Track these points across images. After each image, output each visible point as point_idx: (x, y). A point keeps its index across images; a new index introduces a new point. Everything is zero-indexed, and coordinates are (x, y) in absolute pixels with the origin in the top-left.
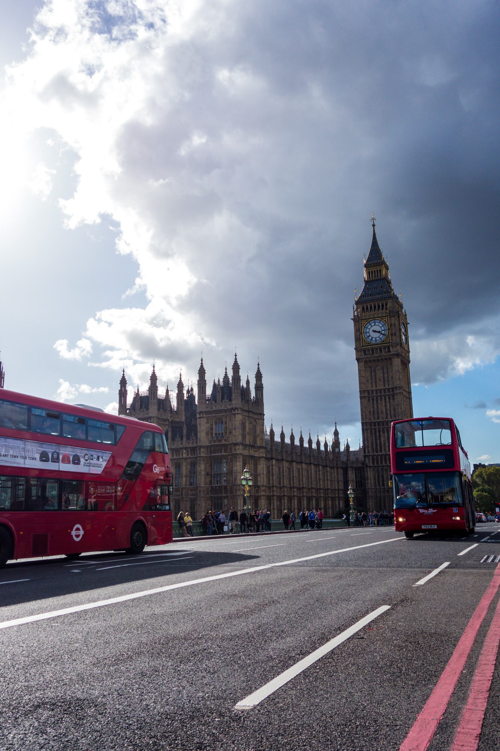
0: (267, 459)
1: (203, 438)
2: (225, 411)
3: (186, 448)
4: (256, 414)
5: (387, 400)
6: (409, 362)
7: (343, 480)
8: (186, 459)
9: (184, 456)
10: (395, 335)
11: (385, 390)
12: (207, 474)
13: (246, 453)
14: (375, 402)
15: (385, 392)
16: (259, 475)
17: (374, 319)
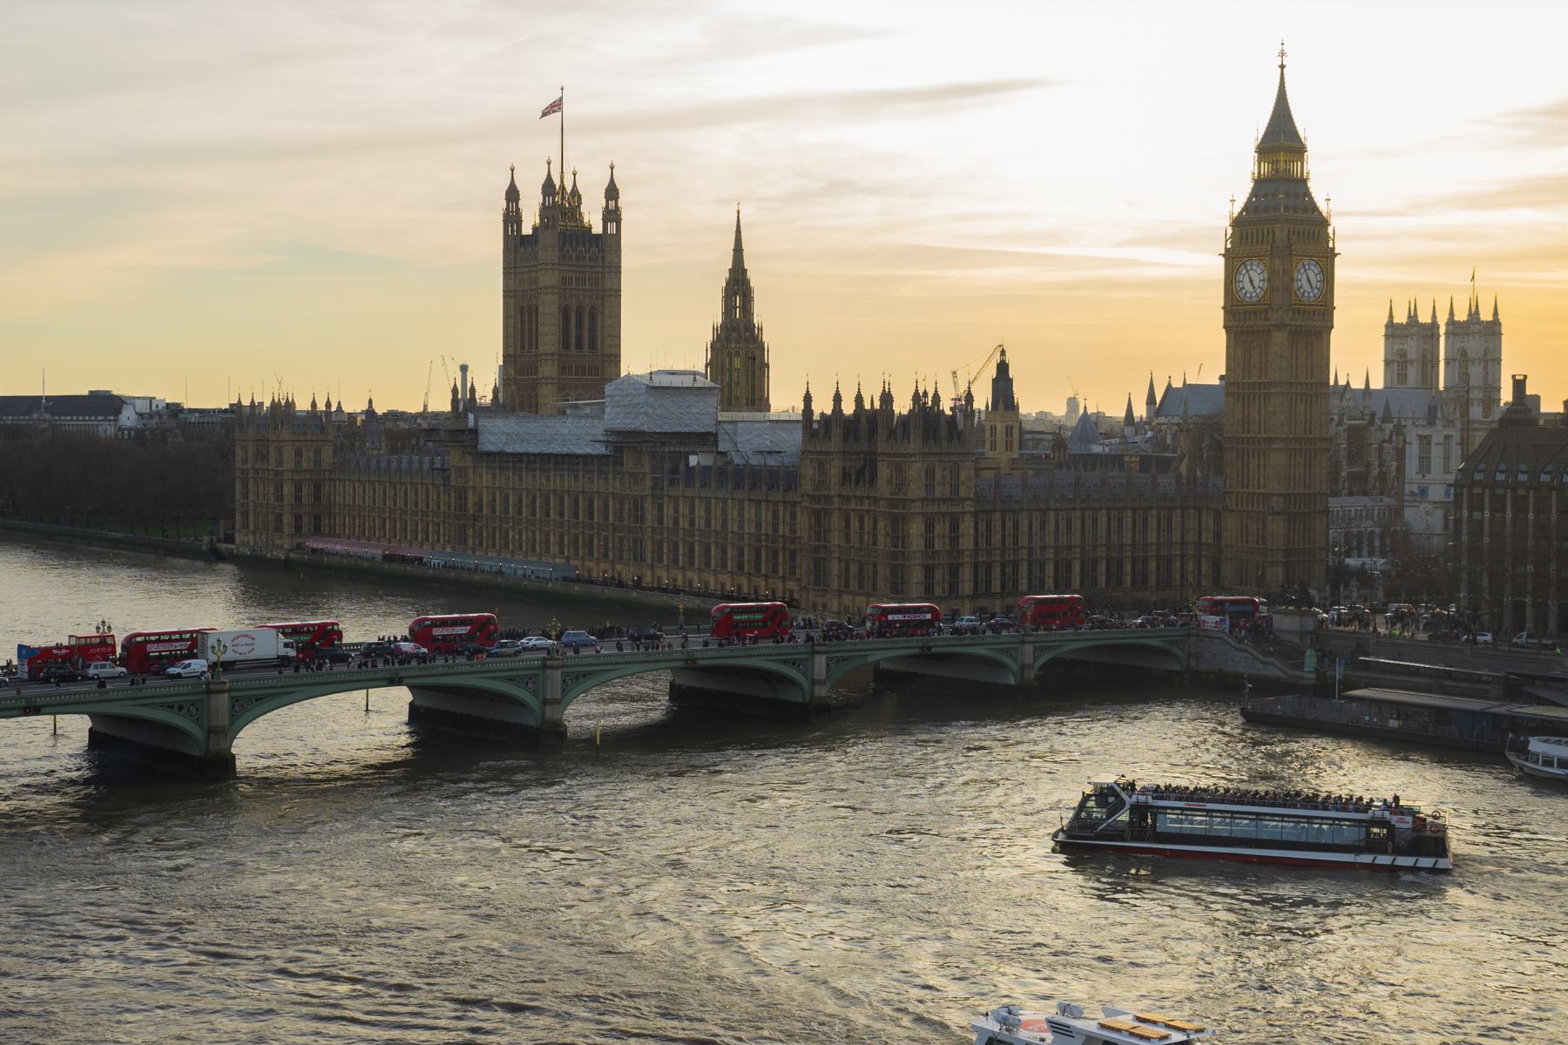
0: (976, 513)
1: (883, 487)
2: (906, 455)
3: (868, 498)
4: (959, 454)
5: (1262, 401)
6: (1332, 327)
7: (1197, 527)
8: (868, 511)
9: (866, 507)
10: (1278, 291)
11: (1260, 383)
12: (888, 534)
13: (934, 509)
14: (1246, 404)
15: (1260, 389)
16: (963, 535)
17: (1250, 257)
